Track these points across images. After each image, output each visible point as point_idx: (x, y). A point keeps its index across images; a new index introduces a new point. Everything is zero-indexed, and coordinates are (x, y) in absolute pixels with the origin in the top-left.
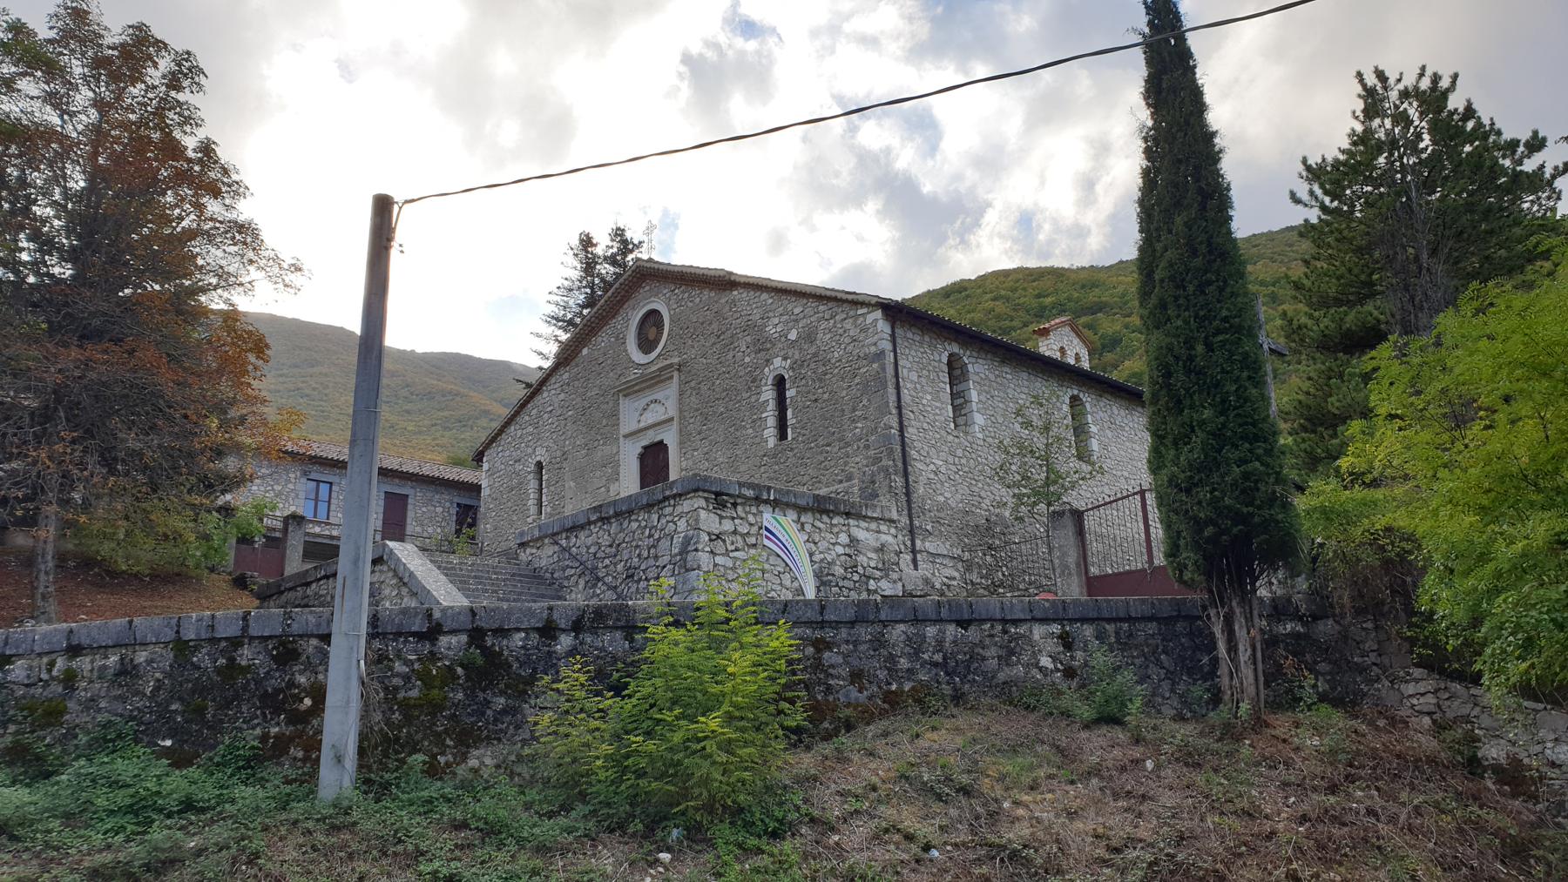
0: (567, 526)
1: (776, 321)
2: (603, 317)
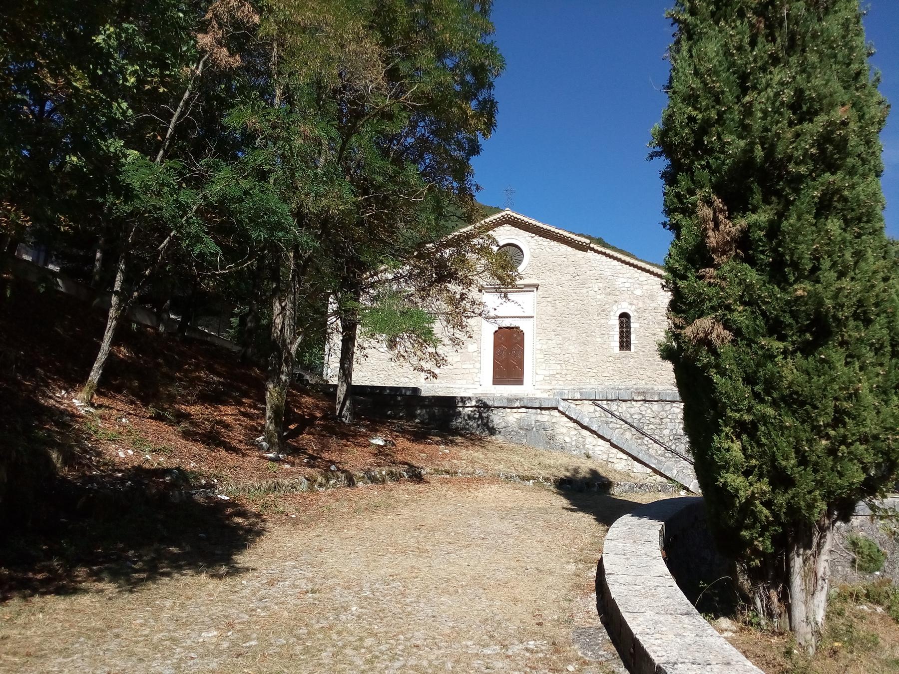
0: (609, 398)
1: (625, 280)
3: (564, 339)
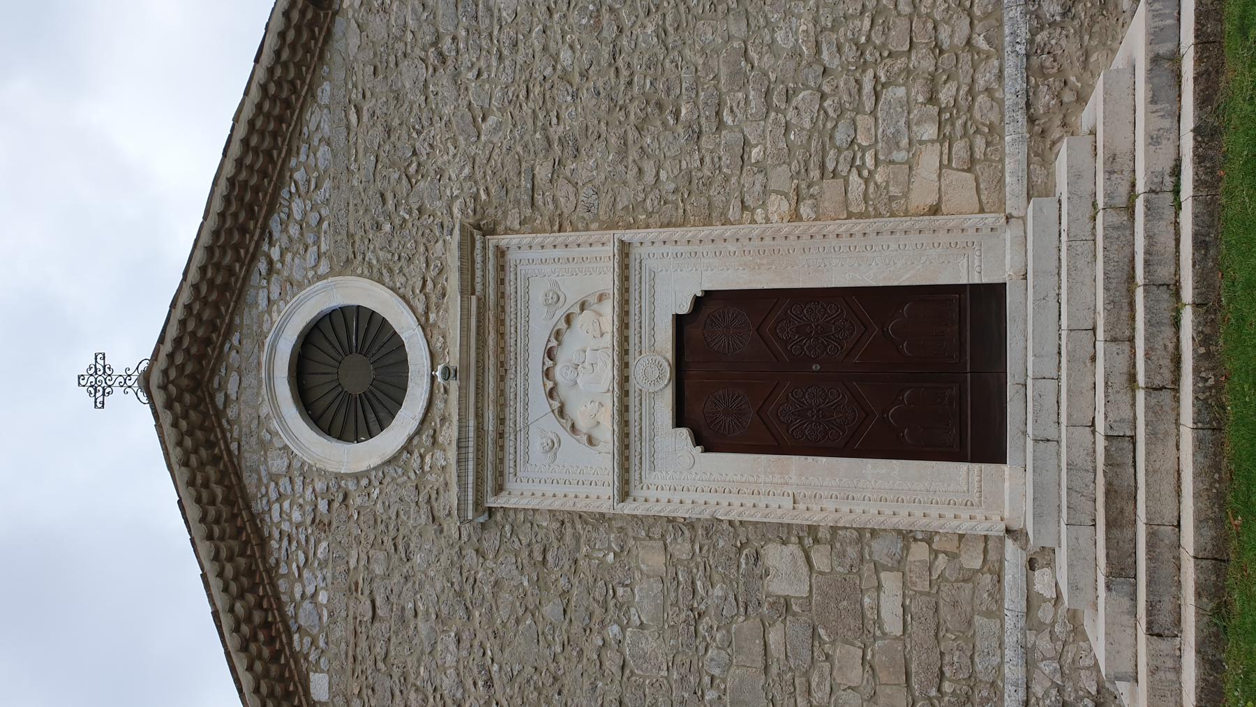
2: (250, 573)
3: (739, 80)
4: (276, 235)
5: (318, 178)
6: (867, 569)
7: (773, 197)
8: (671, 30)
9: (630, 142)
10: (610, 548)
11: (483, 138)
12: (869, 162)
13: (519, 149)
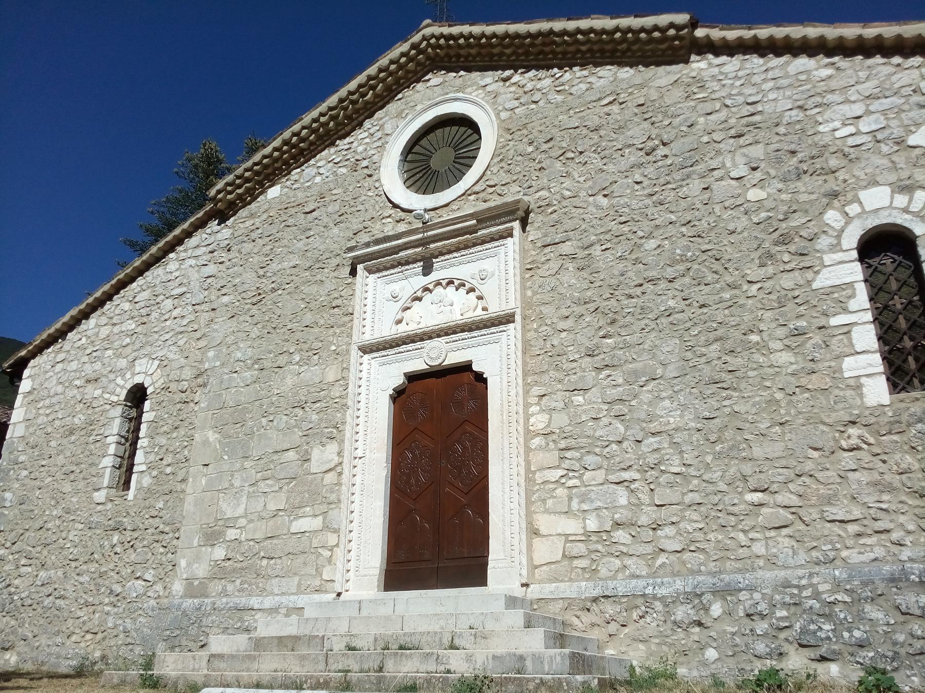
1: (858, 109)
2: (328, 132)
4: (526, 75)
5: (565, 90)
6: (324, 508)
7: (547, 416)
8: (671, 319)
9: (587, 306)
10: (338, 346)
11: (592, 198)
12: (571, 483)
13: (583, 227)
